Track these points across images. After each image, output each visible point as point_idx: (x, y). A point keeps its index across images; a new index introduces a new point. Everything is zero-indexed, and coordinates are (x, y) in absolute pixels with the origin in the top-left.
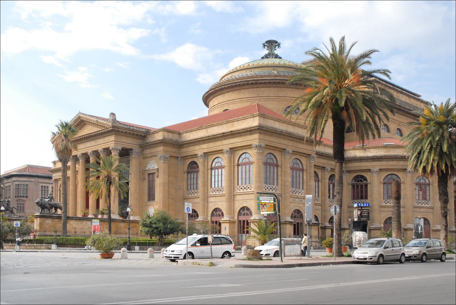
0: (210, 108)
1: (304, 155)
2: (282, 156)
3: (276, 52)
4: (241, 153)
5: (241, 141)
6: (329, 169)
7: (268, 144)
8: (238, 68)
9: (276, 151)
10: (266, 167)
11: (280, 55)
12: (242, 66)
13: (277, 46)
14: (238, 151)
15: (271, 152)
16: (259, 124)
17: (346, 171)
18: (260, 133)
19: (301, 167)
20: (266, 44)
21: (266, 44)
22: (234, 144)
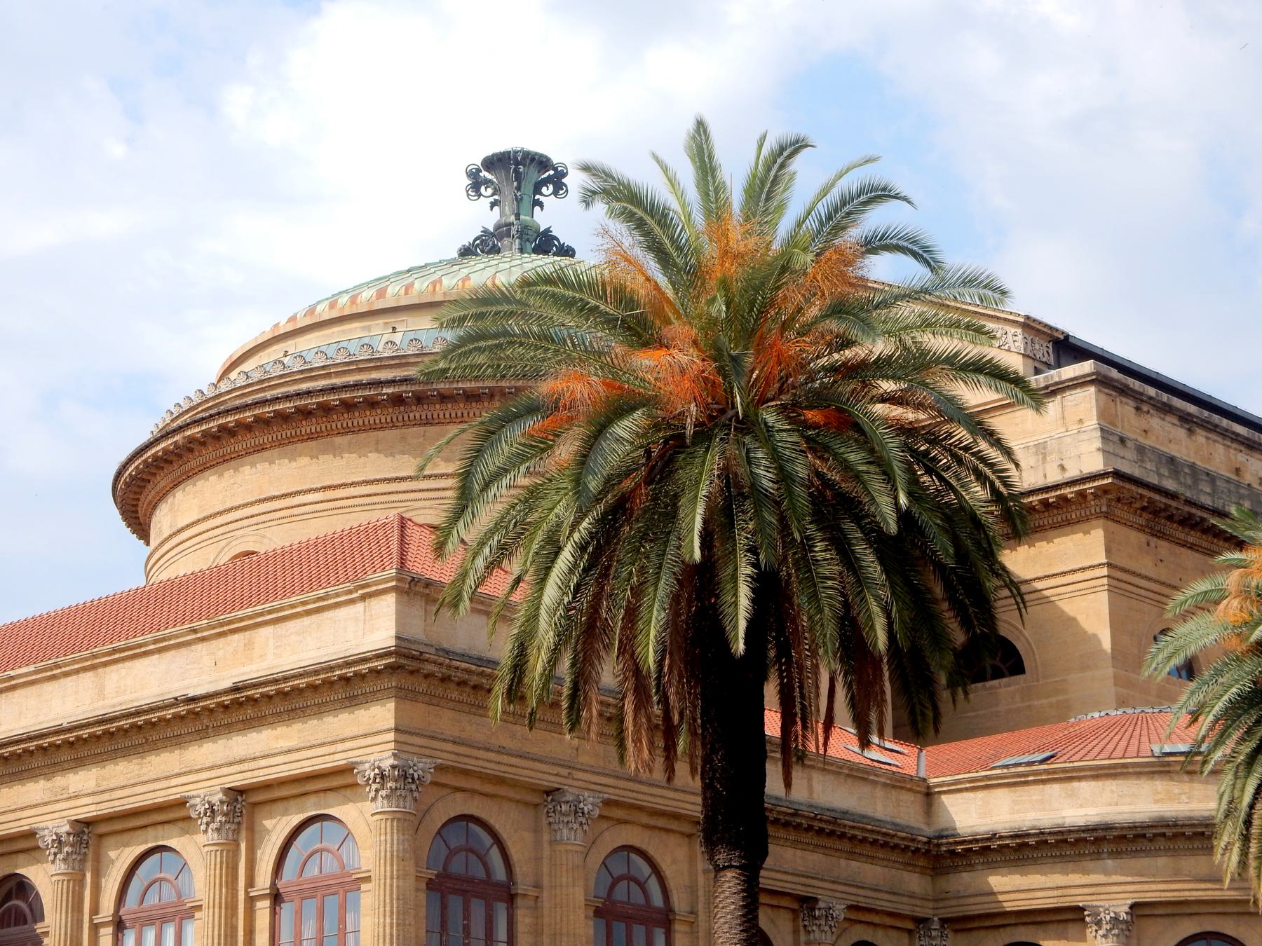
0: (154, 541)
2: (537, 831)
3: (542, 219)
5: (293, 743)
6: (839, 910)
7: (450, 760)
8: (319, 308)
10: (444, 907)
11: (565, 238)
12: (344, 299)
13: (545, 182)
16: (397, 638)
17: (944, 921)
18: (403, 695)
19: (658, 901)
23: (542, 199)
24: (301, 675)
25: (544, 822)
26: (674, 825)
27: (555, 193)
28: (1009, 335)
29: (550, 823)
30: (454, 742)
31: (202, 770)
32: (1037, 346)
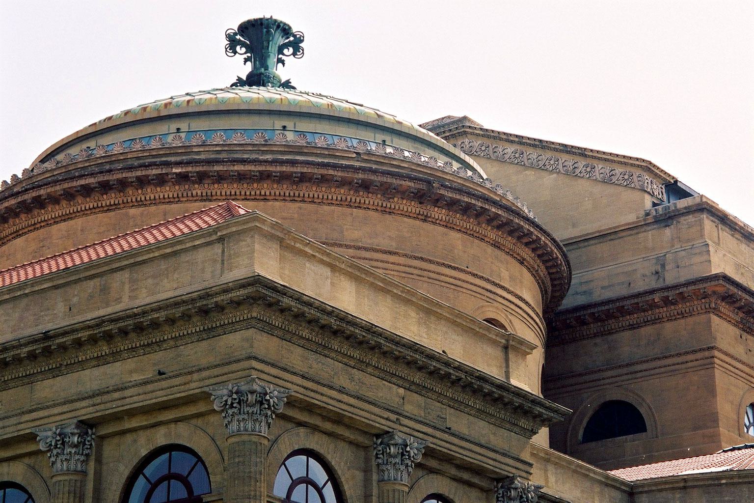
1: (476, 480)
2: (367, 471)
3: (282, 73)
4: (144, 452)
9: (342, 444)
13: (286, 46)
14: (129, 438)
15: (314, 442)
20: (238, 37)
21: (238, 37)
22: (106, 398)
23: (284, 58)
24: (159, 309)
25: (374, 463)
26: (476, 480)
27: (294, 54)
28: (635, 177)
29: (378, 465)
30: (303, 377)
31: (54, 406)
32: (655, 187)
